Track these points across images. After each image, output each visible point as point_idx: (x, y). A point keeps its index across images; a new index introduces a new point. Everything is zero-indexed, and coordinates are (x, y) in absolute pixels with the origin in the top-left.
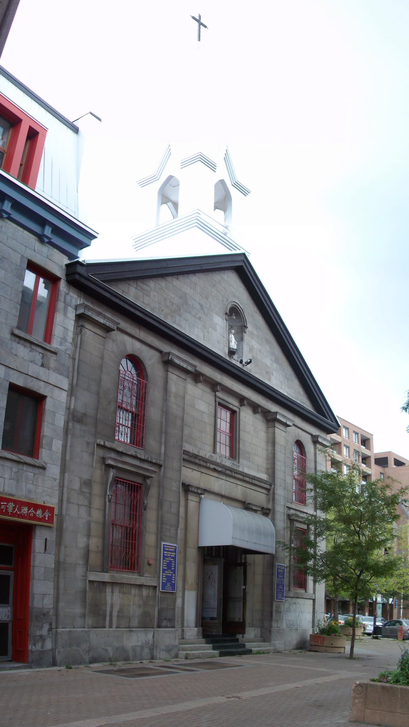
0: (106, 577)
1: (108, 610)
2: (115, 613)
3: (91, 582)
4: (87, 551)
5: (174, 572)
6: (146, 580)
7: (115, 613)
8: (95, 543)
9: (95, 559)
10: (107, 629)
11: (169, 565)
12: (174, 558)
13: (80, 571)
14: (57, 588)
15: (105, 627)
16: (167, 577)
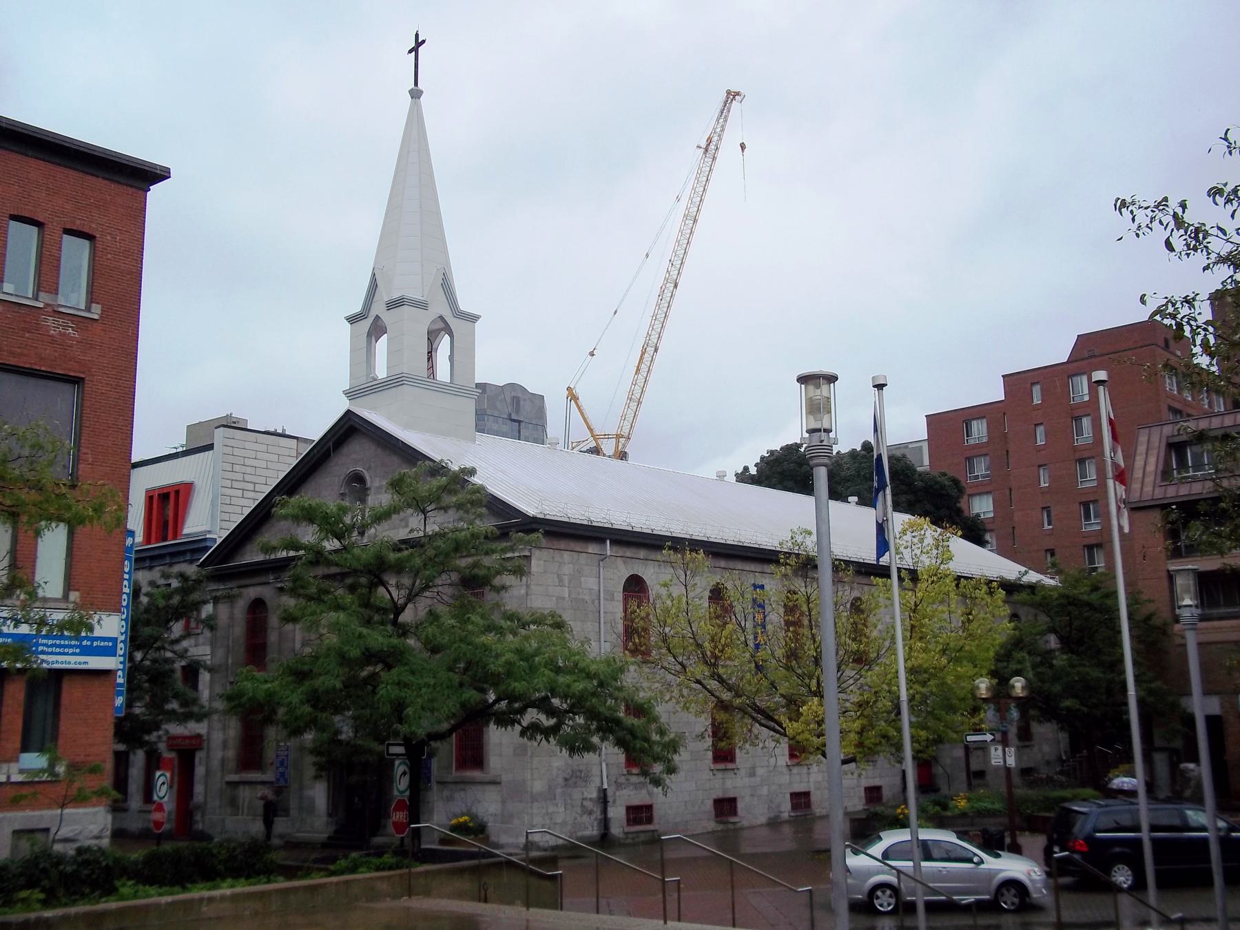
0: (234, 777)
1: (241, 802)
2: (246, 804)
3: (228, 783)
4: (223, 761)
5: (287, 767)
6: (269, 776)
7: (246, 804)
8: (231, 753)
9: (232, 765)
10: (240, 817)
11: (282, 763)
12: (287, 756)
13: (219, 775)
14: (206, 788)
15: (238, 815)
16: (280, 773)
